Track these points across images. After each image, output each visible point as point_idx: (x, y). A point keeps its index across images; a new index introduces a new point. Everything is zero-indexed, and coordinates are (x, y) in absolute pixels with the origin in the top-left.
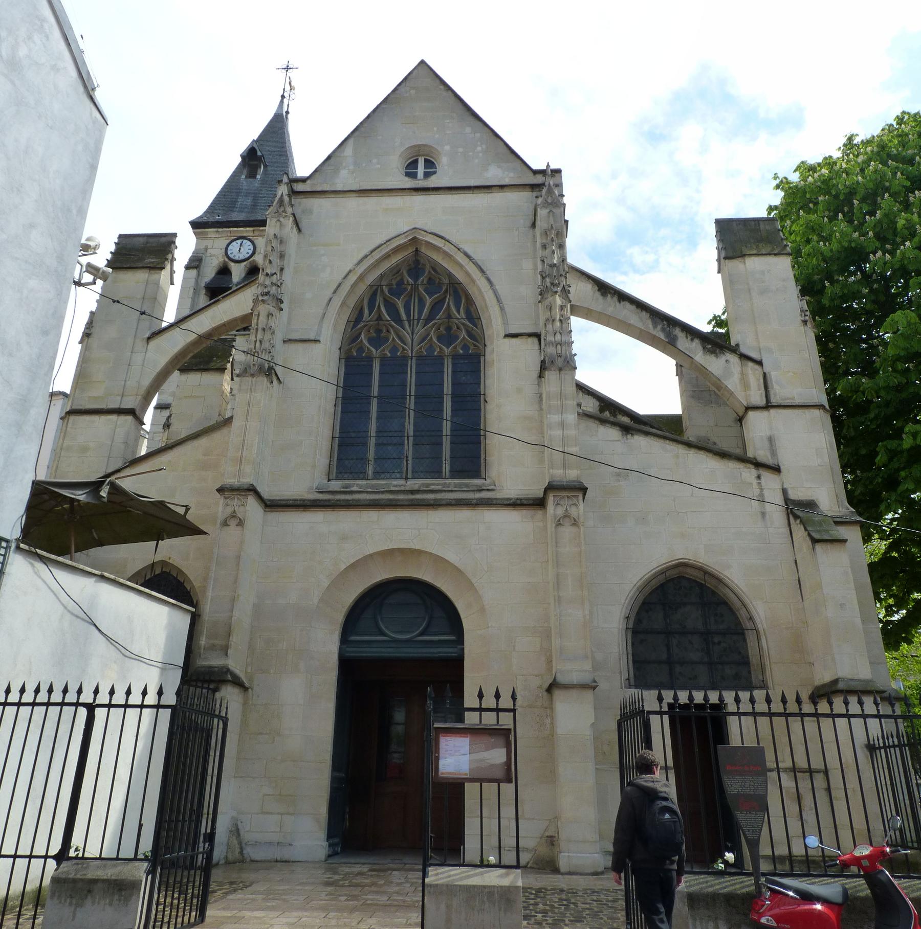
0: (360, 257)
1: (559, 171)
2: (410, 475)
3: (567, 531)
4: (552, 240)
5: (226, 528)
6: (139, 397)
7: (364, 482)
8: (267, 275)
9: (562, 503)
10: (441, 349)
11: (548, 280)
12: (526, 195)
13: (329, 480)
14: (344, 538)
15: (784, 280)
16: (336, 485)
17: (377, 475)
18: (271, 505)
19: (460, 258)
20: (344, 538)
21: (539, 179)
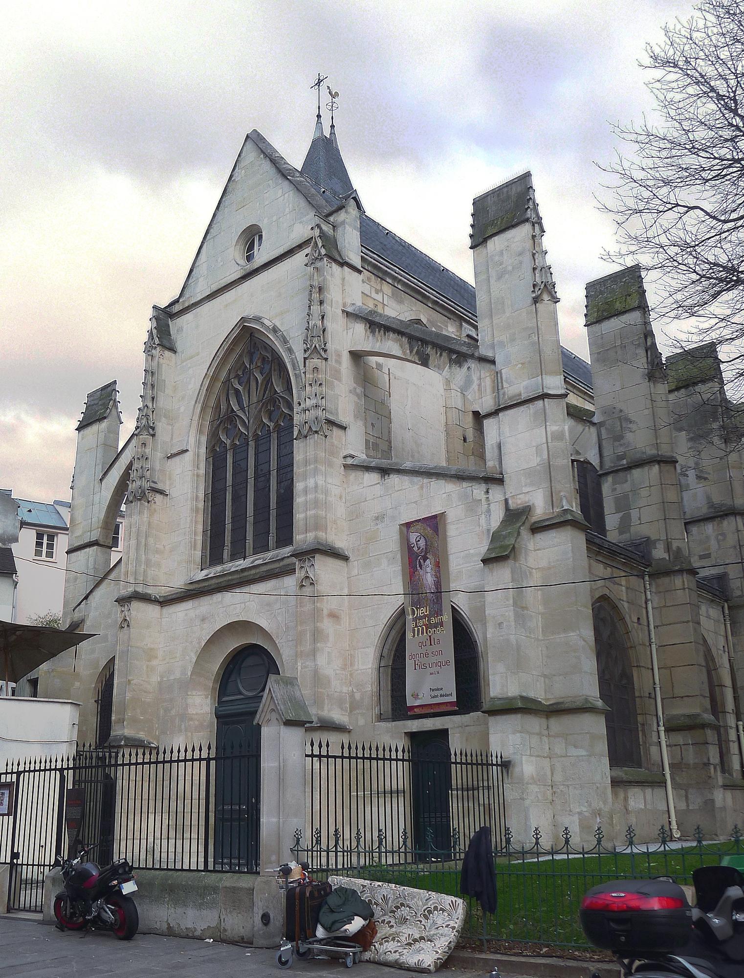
15: (520, 254)
16: (202, 575)
17: (233, 557)
18: (165, 602)
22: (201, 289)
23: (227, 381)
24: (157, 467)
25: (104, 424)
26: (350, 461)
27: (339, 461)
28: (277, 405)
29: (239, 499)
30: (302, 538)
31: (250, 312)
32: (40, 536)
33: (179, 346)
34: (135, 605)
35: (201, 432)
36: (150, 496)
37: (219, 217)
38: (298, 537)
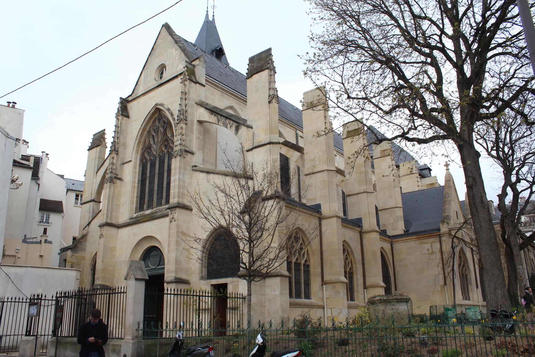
16: (135, 215)
17: (148, 208)
18: (119, 227)
22: (140, 91)
23: (149, 132)
24: (119, 168)
25: (99, 148)
26: (196, 168)
27: (189, 168)
28: (167, 142)
29: (152, 182)
30: (173, 200)
31: (159, 101)
32: (77, 196)
33: (131, 115)
34: (106, 228)
35: (137, 152)
36: (115, 180)
37: (150, 58)
38: (171, 201)
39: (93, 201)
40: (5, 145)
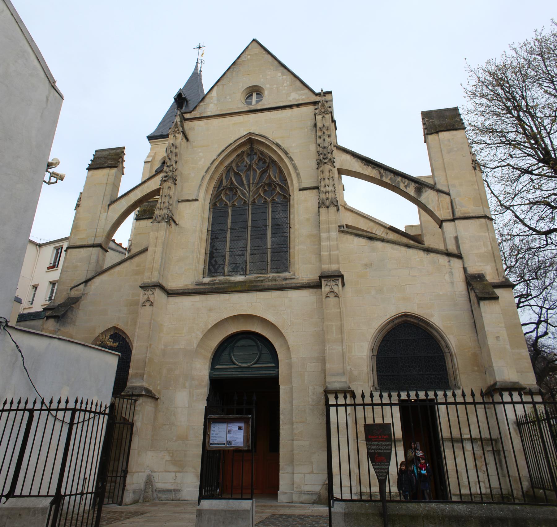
0: (220, 151)
1: (330, 93)
2: (248, 272)
3: (332, 300)
4: (324, 133)
5: (144, 307)
6: (104, 237)
7: (221, 278)
8: (168, 166)
9: (329, 284)
10: (266, 199)
11: (321, 156)
12: (311, 108)
13: (203, 277)
14: (211, 310)
16: (207, 280)
18: (170, 293)
19: (274, 147)
20: (211, 310)
21: (317, 99)
24: (174, 204)
34: (157, 291)
37: (228, 73)
39: (99, 246)
40: (47, 100)
